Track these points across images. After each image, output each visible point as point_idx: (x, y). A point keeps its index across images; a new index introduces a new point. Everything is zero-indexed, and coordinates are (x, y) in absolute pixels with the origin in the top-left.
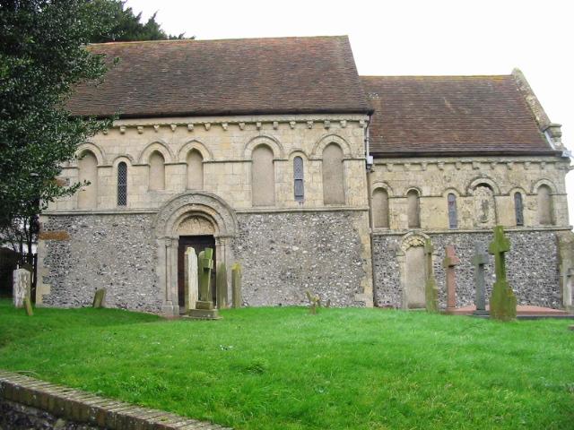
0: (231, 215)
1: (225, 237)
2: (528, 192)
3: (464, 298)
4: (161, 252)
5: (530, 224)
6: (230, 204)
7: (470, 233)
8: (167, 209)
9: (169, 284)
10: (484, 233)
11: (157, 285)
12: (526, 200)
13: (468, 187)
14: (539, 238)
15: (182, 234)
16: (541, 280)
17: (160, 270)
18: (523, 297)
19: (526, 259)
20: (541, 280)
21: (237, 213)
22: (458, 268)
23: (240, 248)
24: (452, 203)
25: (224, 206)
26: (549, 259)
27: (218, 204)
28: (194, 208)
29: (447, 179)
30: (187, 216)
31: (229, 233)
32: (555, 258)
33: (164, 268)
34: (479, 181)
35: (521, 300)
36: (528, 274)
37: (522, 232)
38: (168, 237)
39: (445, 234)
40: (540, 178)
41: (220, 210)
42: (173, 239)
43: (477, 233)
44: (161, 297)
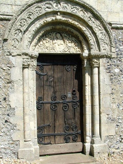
0: (105, 29)
1: (102, 57)
4: (16, 73)
6: (104, 16)
8: (24, 15)
9: (27, 118)
11: (11, 120)
15: (41, 51)
17: (15, 99)
21: (113, 28)
23: (117, 71)
25: (97, 17)
27: (89, 15)
28: (59, 17)
30: (48, 28)
31: (103, 52)
33: (21, 96)
38: (26, 54)
41: (94, 24)
42: (32, 57)
44: (16, 136)
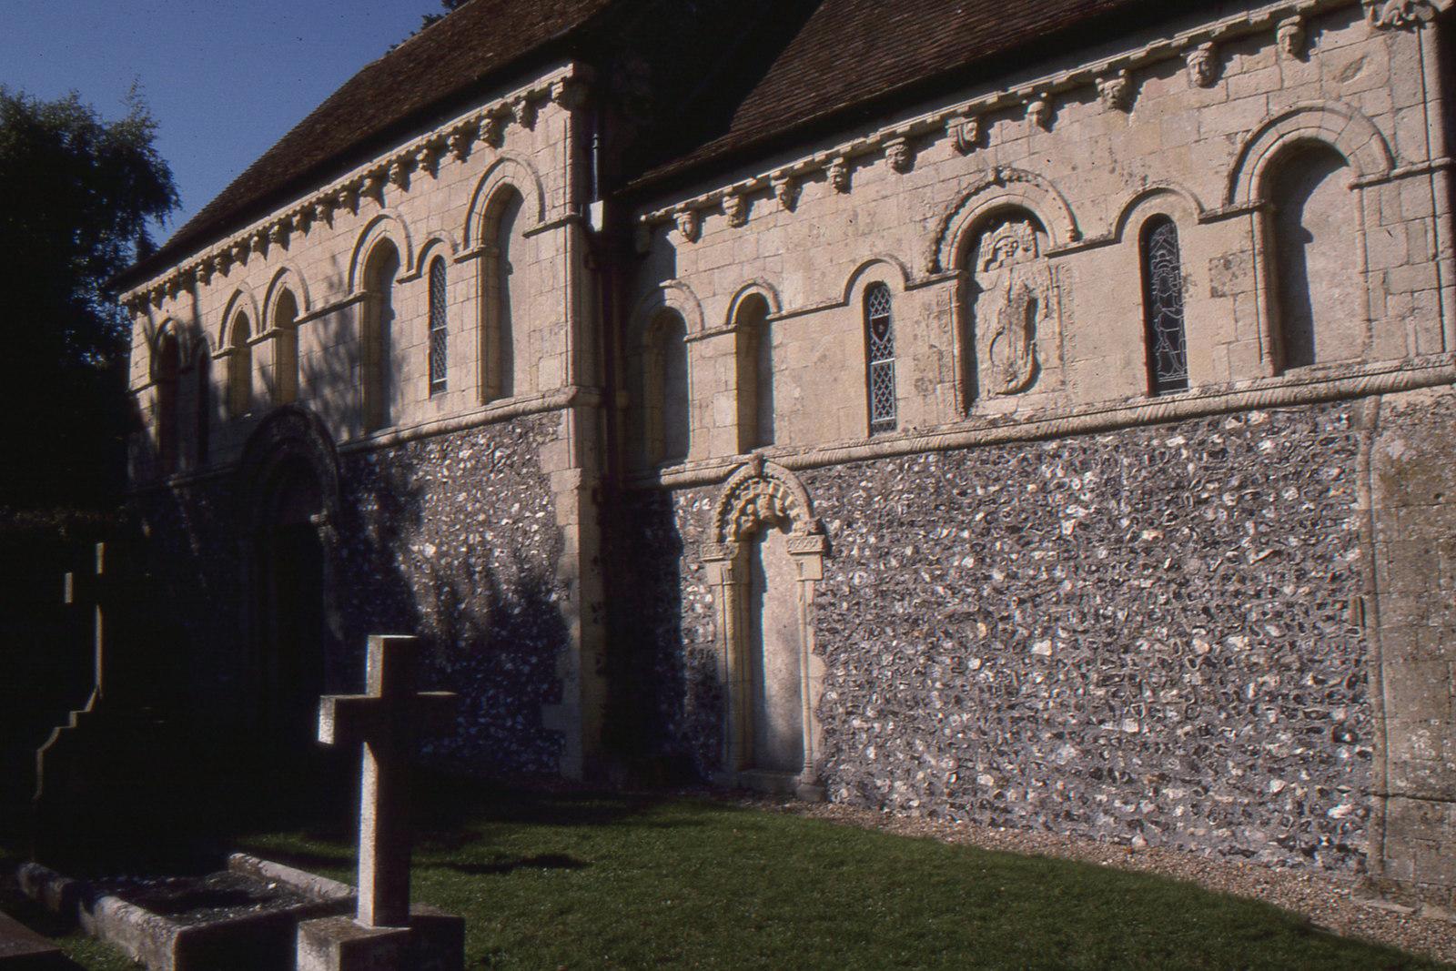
2: (1215, 203)
3: (919, 745)
5: (1220, 376)
7: (943, 450)
10: (999, 443)
12: (1197, 250)
13: (939, 240)
14: (1267, 445)
16: (1271, 680)
18: (1174, 765)
19: (1193, 564)
20: (1271, 680)
22: (899, 608)
24: (878, 330)
26: (1325, 559)
29: (863, 219)
32: (1352, 555)
34: (978, 205)
35: (1164, 778)
36: (1201, 646)
37: (1173, 422)
39: (854, 463)
40: (1276, 111)
43: (971, 446)
